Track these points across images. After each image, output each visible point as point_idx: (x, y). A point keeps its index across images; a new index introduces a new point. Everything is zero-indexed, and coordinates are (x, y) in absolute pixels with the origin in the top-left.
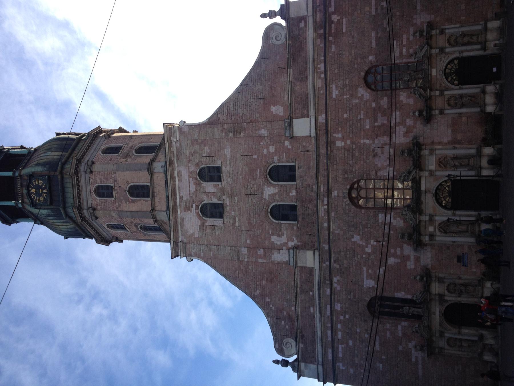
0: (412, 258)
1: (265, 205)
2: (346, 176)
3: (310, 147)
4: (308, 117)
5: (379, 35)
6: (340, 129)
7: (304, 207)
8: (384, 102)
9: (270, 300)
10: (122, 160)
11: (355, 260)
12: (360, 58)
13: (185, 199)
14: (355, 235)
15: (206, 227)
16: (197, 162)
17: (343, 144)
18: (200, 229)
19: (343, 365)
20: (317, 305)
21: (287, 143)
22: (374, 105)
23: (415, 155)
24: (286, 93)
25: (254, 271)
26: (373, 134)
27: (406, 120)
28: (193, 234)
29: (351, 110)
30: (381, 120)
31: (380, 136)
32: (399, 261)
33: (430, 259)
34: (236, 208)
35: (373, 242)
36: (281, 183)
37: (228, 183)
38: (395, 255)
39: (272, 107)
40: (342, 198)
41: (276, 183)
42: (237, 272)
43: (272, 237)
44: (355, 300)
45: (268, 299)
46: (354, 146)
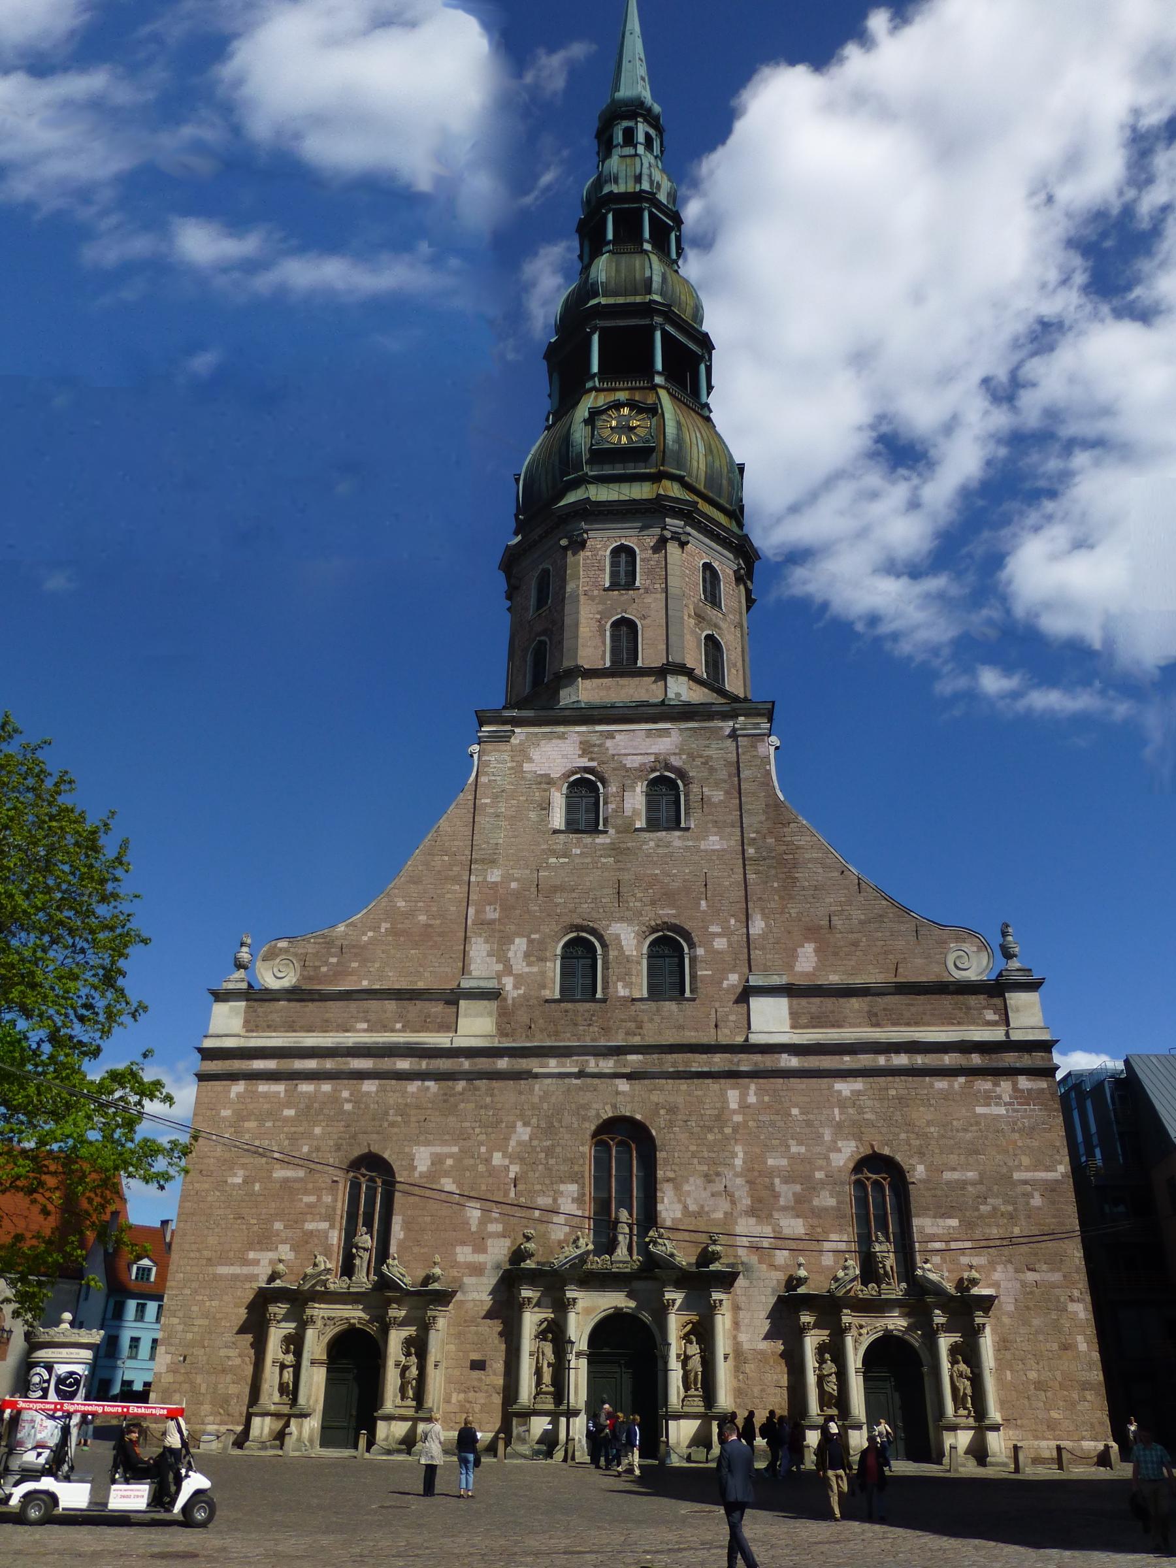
0: (481, 1258)
1: (596, 926)
2: (662, 1112)
3: (727, 1031)
4: (792, 1027)
5: (970, 1188)
6: (766, 1099)
7: (593, 1015)
8: (826, 1200)
9: (383, 930)
10: (691, 607)
11: (473, 1129)
12: (921, 1145)
13: (609, 743)
14: (529, 1129)
17: (734, 1105)
18: (541, 775)
19: (238, 1095)
20: (373, 1039)
21: (734, 979)
22: (819, 1175)
23: (712, 1267)
24: (844, 977)
25: (449, 896)
26: (756, 1174)
28: (531, 760)
29: (809, 1124)
30: (786, 1192)
32: (474, 1229)
33: (478, 1298)
34: (588, 860)
35: (514, 1170)
36: (645, 962)
37: (645, 843)
39: (813, 945)
41: (645, 951)
42: (446, 858)
44: (386, 1124)
45: (385, 926)
46: (728, 1131)
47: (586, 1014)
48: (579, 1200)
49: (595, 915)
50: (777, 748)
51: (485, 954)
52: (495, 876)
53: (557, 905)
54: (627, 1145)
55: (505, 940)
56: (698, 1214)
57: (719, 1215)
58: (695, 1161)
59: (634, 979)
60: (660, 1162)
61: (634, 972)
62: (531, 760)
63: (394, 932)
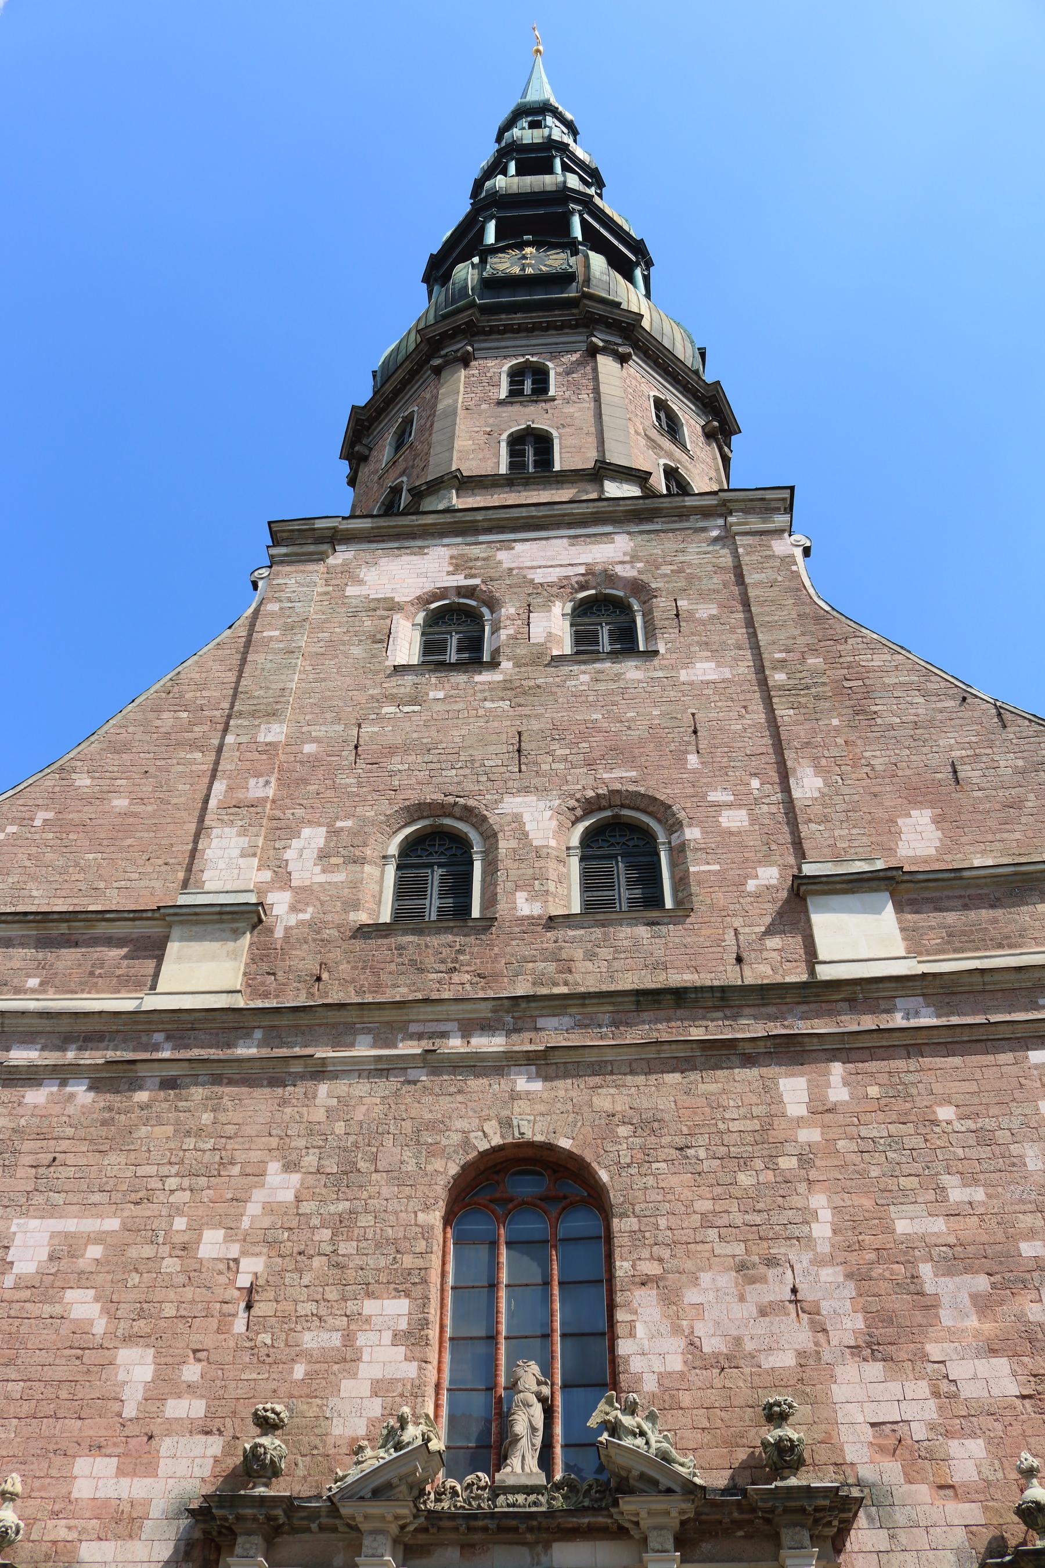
1: (471, 803)
6: (873, 1091)
7: (459, 952)
9: (38, 822)
11: (163, 1178)
14: (295, 1178)
16: (653, 586)
18: (378, 600)
21: (769, 876)
26: (872, 1256)
27: (973, 1435)
28: (361, 582)
29: (984, 1138)
31: (858, 1288)
32: (130, 1411)
34: (461, 706)
35: (252, 1267)
38: (164, 1387)
40: (505, 1113)
42: (185, 715)
43: (323, 830)
45: (41, 816)
47: (446, 952)
48: (412, 1338)
49: (470, 786)
50: (807, 552)
51: (237, 852)
52: (274, 732)
53: (392, 774)
54: (532, 1204)
55: (283, 831)
56: (726, 1363)
57: (787, 1360)
59: (551, 886)
60: (621, 1241)
61: (552, 875)
62: (361, 582)
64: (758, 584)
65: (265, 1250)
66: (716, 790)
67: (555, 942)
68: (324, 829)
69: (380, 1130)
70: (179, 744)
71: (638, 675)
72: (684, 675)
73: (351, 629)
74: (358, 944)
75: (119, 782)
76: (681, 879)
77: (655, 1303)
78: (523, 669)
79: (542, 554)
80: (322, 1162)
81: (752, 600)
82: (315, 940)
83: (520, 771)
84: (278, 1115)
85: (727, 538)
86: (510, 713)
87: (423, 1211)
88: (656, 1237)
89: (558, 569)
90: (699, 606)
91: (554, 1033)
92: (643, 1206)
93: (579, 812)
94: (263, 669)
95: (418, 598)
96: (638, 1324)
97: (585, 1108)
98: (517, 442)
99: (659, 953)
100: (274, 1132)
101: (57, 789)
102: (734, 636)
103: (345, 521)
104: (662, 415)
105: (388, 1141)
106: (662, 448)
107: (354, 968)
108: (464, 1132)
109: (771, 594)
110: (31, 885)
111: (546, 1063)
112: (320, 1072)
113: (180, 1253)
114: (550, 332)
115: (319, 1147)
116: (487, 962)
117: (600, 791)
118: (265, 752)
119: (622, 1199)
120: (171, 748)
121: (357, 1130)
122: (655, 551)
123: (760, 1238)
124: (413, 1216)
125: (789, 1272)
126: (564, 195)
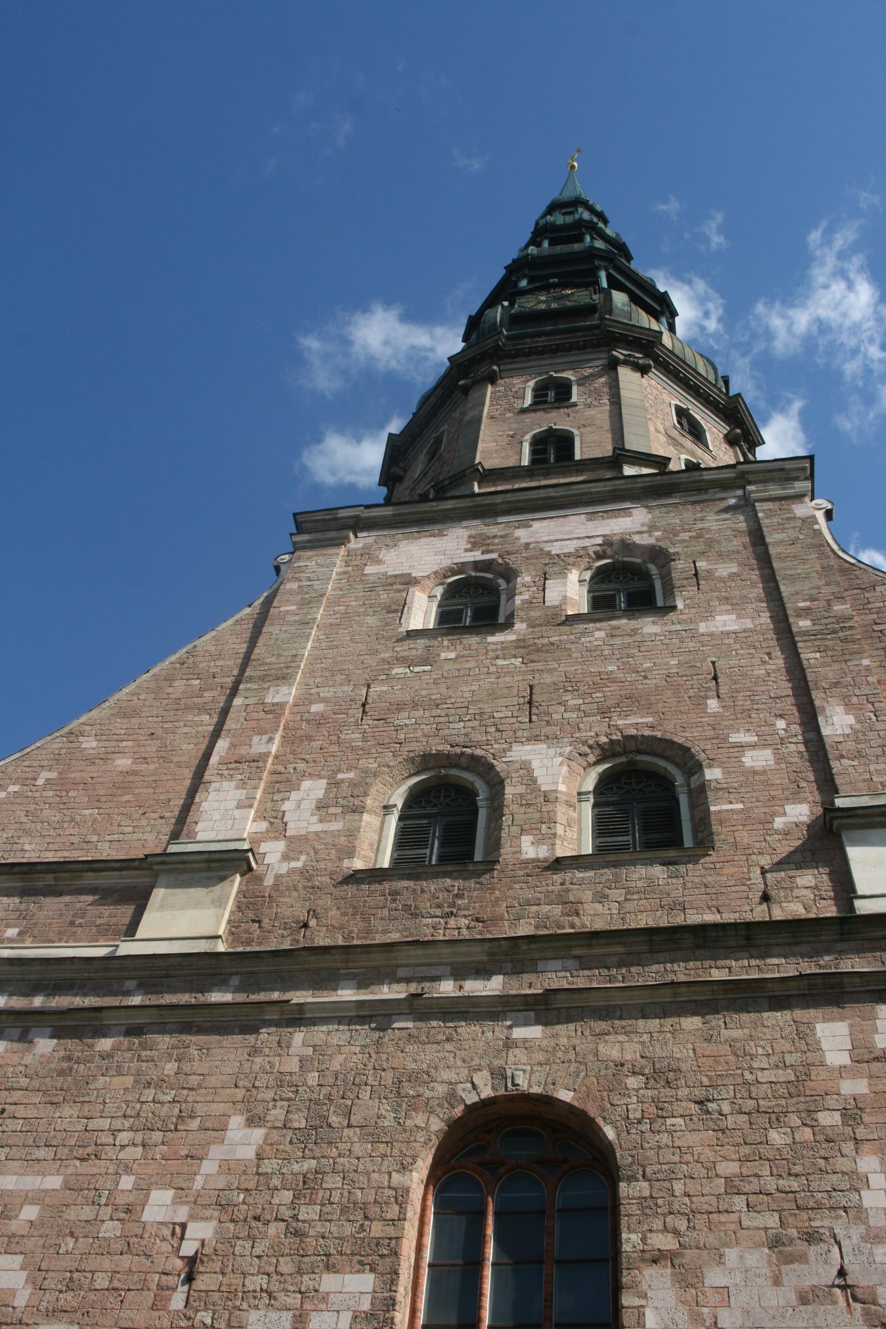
1: (478, 752)
7: (457, 896)
9: (40, 782)
11: (114, 1132)
14: (258, 1134)
15: (399, 591)
16: (672, 551)
18: (395, 576)
21: (800, 812)
28: (379, 562)
34: (472, 664)
40: (498, 1063)
42: (197, 682)
45: (44, 776)
49: (477, 737)
55: (282, 784)
58: (739, 1202)
60: (629, 1209)
61: (561, 817)
62: (379, 562)
63: (60, 785)
64: (780, 543)
65: (216, 1214)
66: (738, 731)
67: (562, 884)
68: (324, 781)
69: (357, 1081)
70: (188, 708)
71: (656, 629)
72: (703, 628)
73: (367, 602)
74: (350, 890)
75: (125, 744)
76: (701, 820)
77: (668, 1284)
78: (537, 629)
79: (561, 529)
80: (290, 1116)
81: (773, 557)
82: (305, 887)
83: (530, 721)
84: (247, 1065)
85: (747, 506)
86: (522, 669)
87: (398, 1171)
88: (670, 1204)
89: (575, 542)
90: (718, 566)
91: (555, 977)
92: (656, 1168)
93: (592, 758)
94: (277, 639)
95: (435, 573)
96: (648, 1312)
97: (590, 1057)
98: (540, 443)
99: (677, 893)
100: (240, 1083)
101: (63, 751)
102: (756, 590)
103: (367, 511)
104: (684, 422)
105: (365, 1094)
106: (684, 447)
107: (344, 914)
108: (451, 1083)
109: (794, 550)
110: (25, 840)
111: (545, 1008)
112: (298, 1018)
113: (122, 1215)
114: (572, 353)
115: (289, 1100)
116: (487, 906)
117: (614, 737)
118: (271, 712)
119: (630, 1159)
120: (180, 712)
121: (331, 1080)
122: (674, 521)
123: (798, 1208)
124: (387, 1176)
125: (836, 1249)
126: (592, 254)
